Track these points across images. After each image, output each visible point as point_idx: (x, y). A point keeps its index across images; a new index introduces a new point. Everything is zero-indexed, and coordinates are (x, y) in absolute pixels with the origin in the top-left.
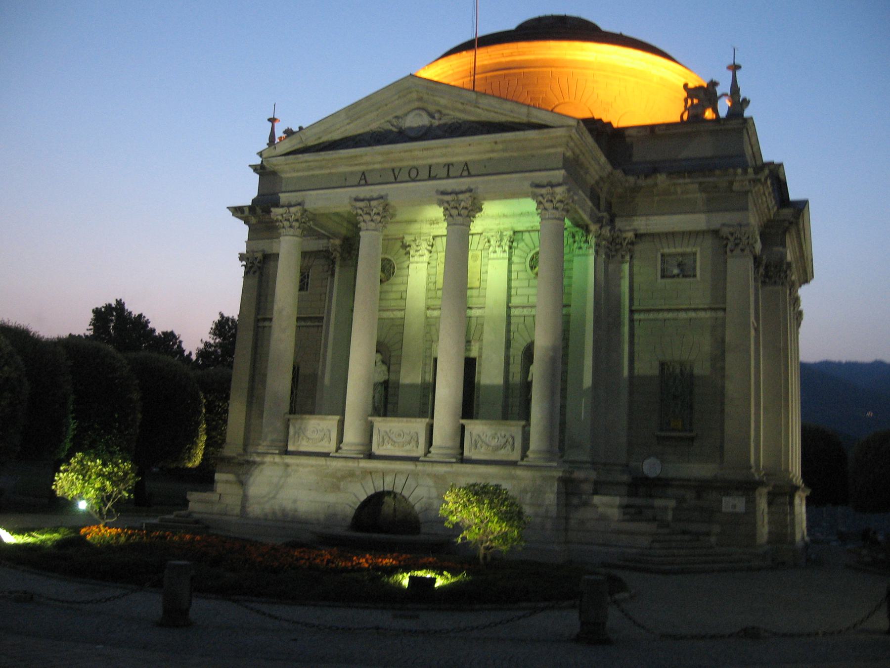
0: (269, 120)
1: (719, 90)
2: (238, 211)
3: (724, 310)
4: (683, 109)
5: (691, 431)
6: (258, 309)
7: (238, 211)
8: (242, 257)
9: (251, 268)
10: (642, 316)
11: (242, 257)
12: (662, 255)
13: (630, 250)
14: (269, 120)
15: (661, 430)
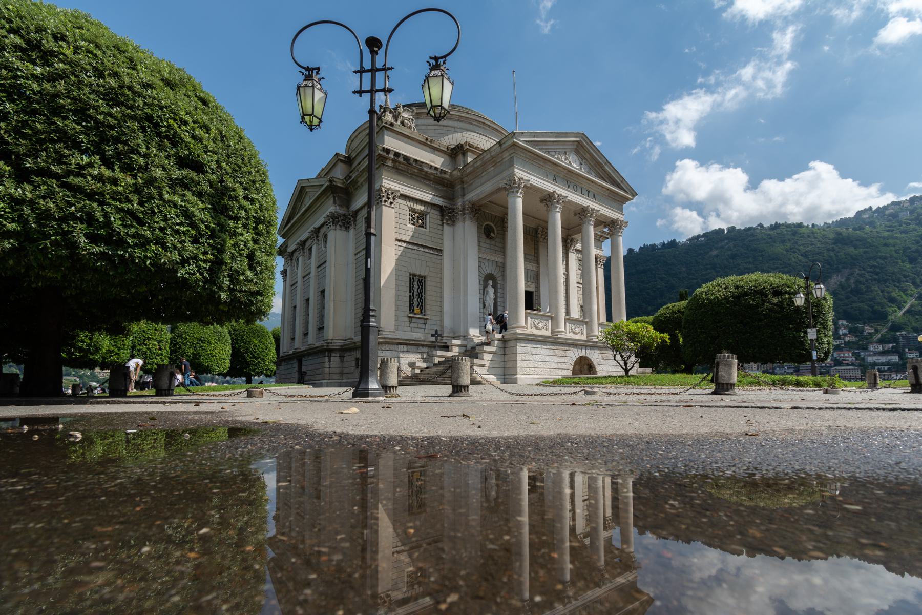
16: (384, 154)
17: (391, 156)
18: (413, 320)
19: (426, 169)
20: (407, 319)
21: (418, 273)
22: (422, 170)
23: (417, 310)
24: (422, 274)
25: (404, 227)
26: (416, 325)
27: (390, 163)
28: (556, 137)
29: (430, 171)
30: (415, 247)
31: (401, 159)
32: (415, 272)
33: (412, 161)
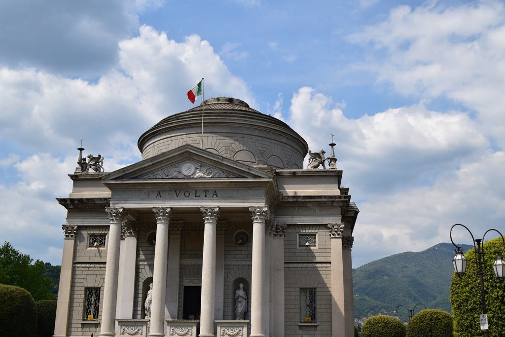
0: (79, 149)
1: (326, 156)
2: (63, 201)
3: (330, 263)
4: (308, 163)
5: (315, 323)
6: (74, 257)
7: (63, 201)
8: (64, 227)
9: (69, 233)
10: (290, 265)
11: (64, 227)
12: (299, 235)
13: (283, 232)
14: (79, 149)
15: (301, 322)
16: (63, 203)
17: (68, 202)
18: (85, 325)
19: (97, 202)
20: (80, 325)
21: (93, 286)
22: (95, 203)
23: (91, 317)
24: (96, 286)
25: (84, 251)
26: (87, 330)
27: (71, 207)
28: (151, 161)
29: (101, 202)
30: (92, 265)
31: (76, 202)
32: (89, 286)
33: (85, 201)
